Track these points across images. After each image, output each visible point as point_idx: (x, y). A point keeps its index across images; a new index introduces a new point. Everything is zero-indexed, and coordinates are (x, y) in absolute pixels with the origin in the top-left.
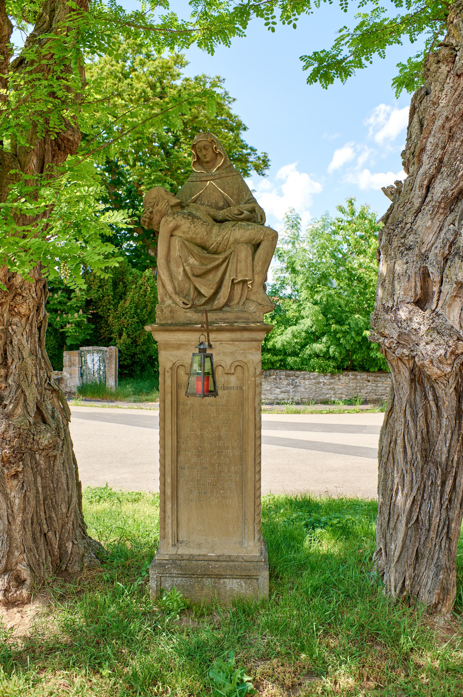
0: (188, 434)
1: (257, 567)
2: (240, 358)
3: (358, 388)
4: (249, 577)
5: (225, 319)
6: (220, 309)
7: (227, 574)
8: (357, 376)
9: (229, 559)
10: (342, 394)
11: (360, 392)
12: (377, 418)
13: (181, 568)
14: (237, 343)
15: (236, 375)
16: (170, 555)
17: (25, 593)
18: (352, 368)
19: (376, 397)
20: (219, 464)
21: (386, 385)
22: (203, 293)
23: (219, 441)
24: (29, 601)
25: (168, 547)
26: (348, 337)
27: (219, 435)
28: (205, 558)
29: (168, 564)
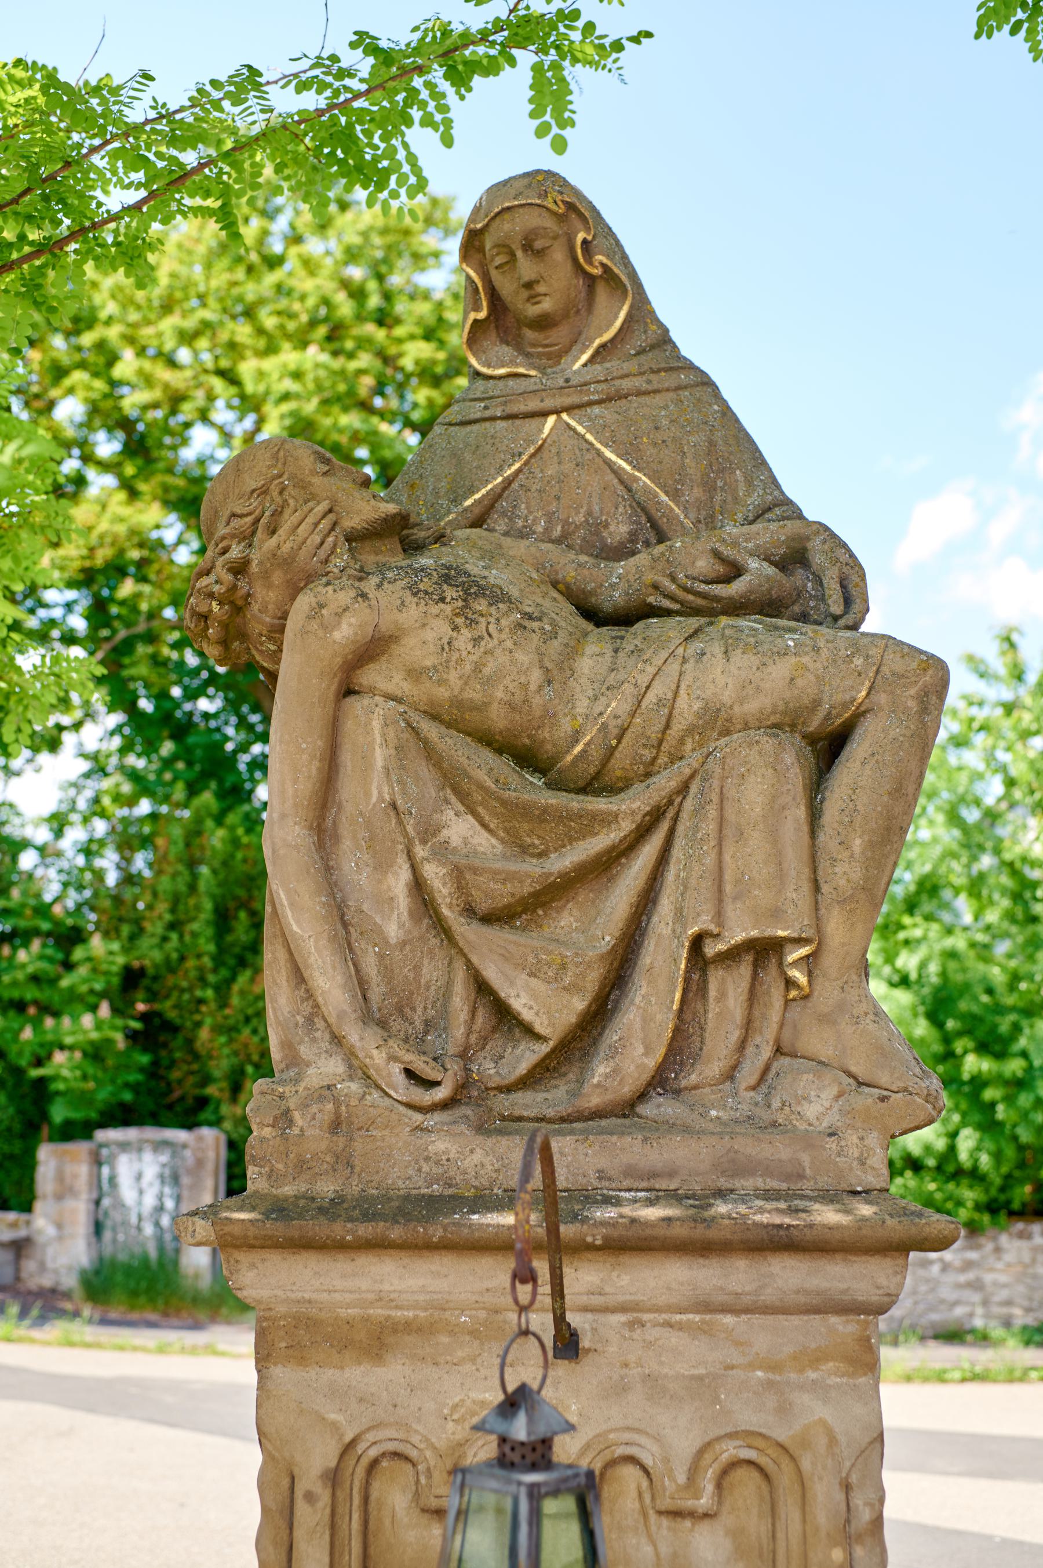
2: (749, 1418)
5: (653, 1175)
10: (1009, 1303)
14: (729, 1320)
15: (726, 1519)
22: (527, 1015)
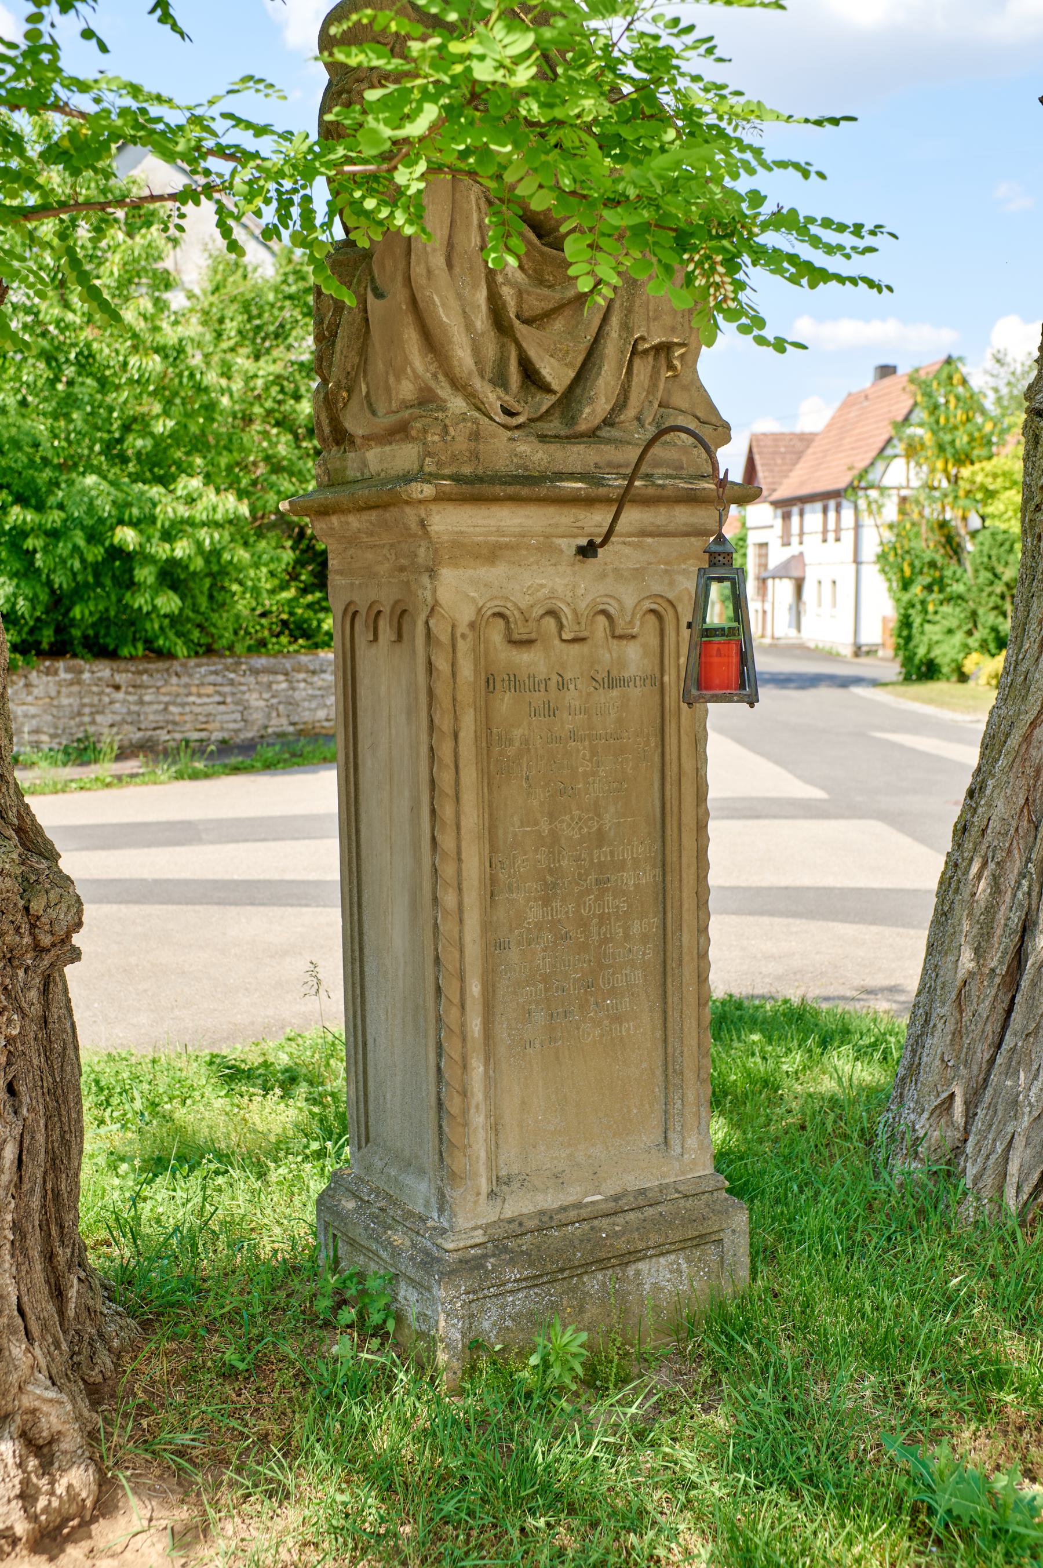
0: (515, 835)
1: (717, 1207)
2: (657, 588)
3: (87, 710)
4: (700, 1241)
5: (619, 466)
6: (592, 435)
7: (651, 1244)
8: (81, 672)
9: (644, 1199)
10: (37, 731)
11: (93, 722)
12: (318, 791)
13: (529, 1258)
14: (649, 540)
15: (640, 639)
16: (486, 1228)
17: (77, 1479)
18: (60, 650)
19: (139, 735)
20: (601, 917)
21: (166, 699)
22: (549, 379)
23: (600, 846)
24: (105, 1504)
25: (476, 1202)
26: (63, 548)
27: (599, 830)
28: (584, 1213)
29: (485, 1256)
